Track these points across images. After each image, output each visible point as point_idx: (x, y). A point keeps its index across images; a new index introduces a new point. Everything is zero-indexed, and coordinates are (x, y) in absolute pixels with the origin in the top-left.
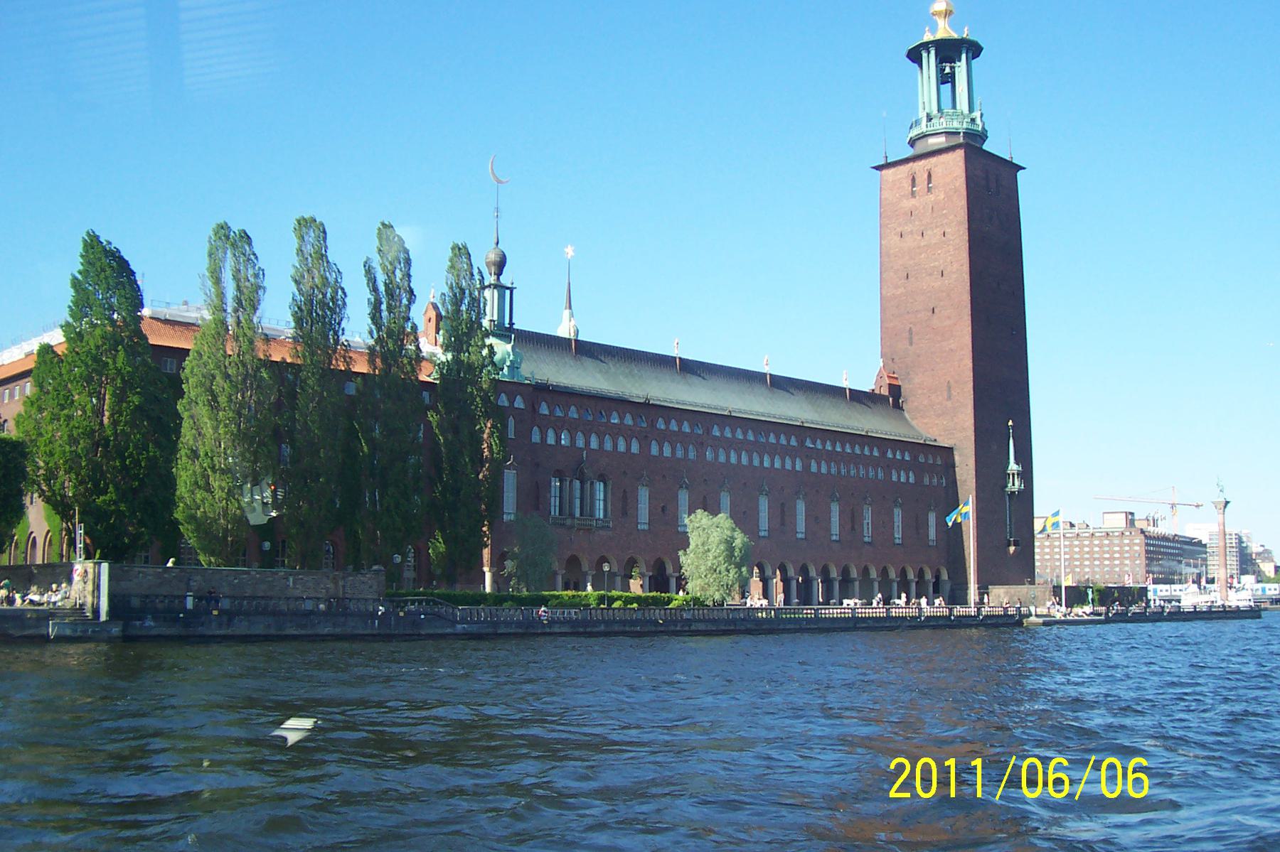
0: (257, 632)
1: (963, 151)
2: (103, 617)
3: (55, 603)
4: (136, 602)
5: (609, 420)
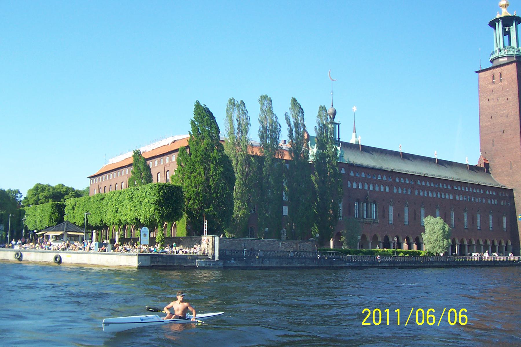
0: (273, 266)
1: (516, 64)
2: (216, 259)
3: (196, 253)
4: (228, 253)
5: (377, 178)
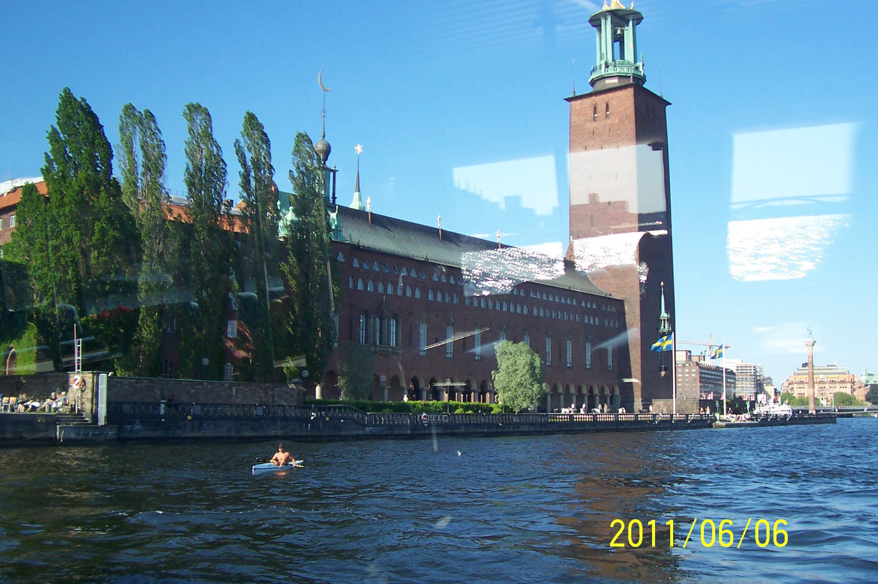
0: (221, 434)
2: (102, 422)
3: (56, 409)
4: (127, 408)
